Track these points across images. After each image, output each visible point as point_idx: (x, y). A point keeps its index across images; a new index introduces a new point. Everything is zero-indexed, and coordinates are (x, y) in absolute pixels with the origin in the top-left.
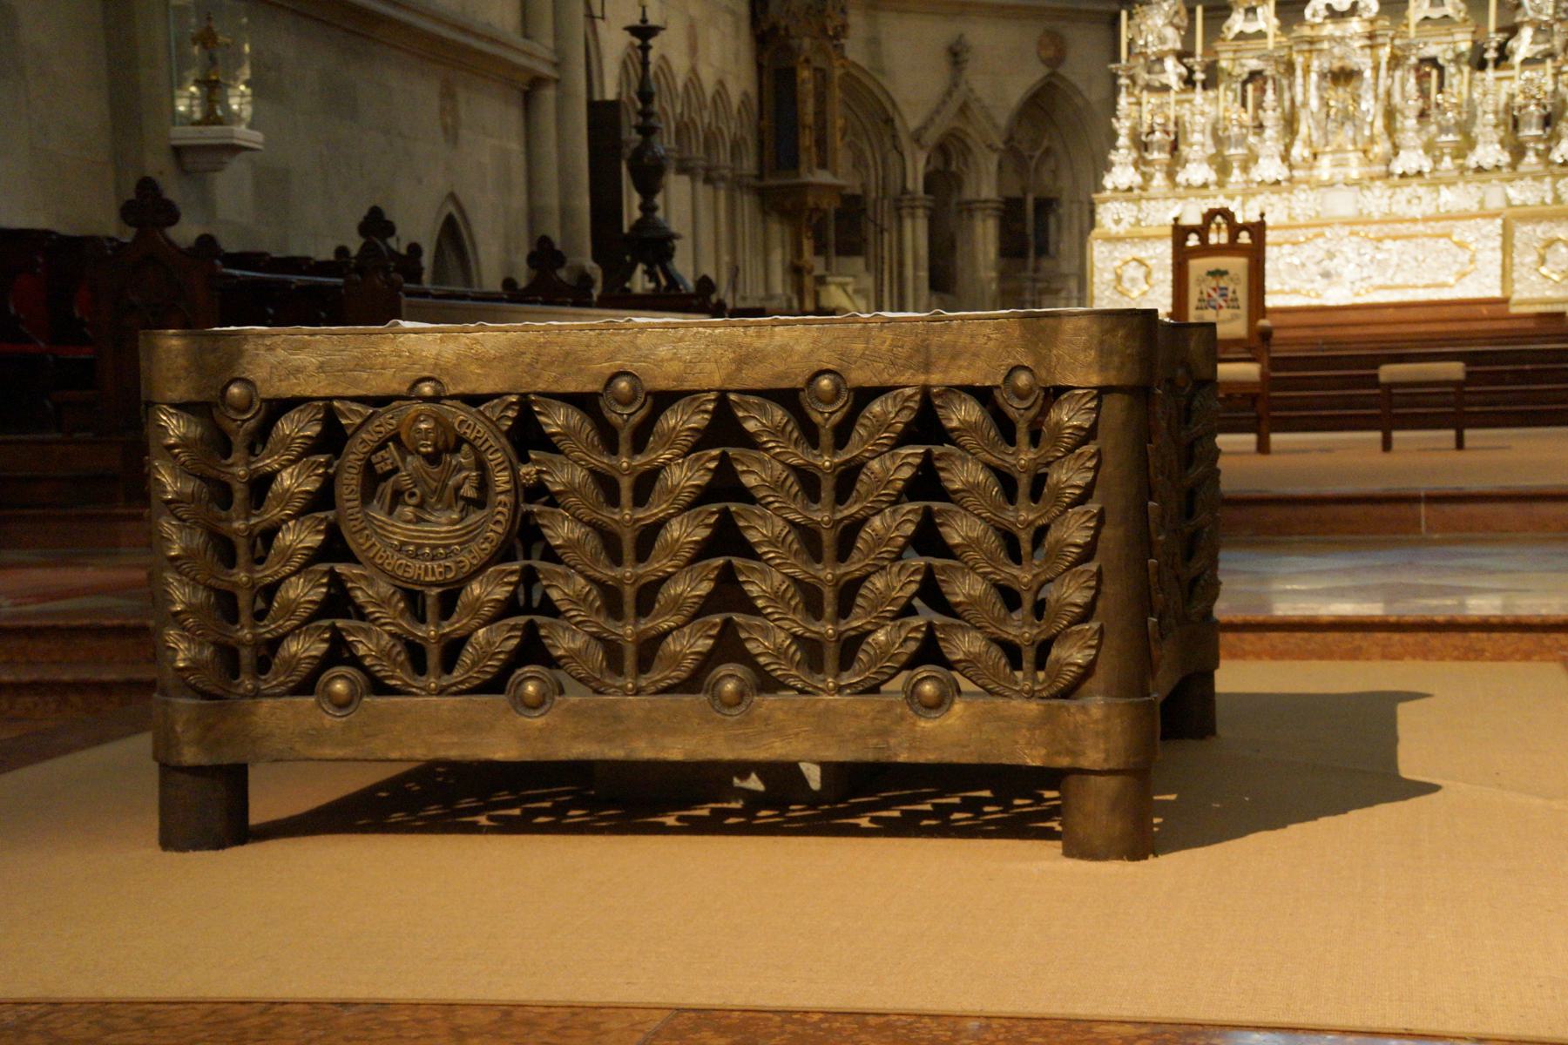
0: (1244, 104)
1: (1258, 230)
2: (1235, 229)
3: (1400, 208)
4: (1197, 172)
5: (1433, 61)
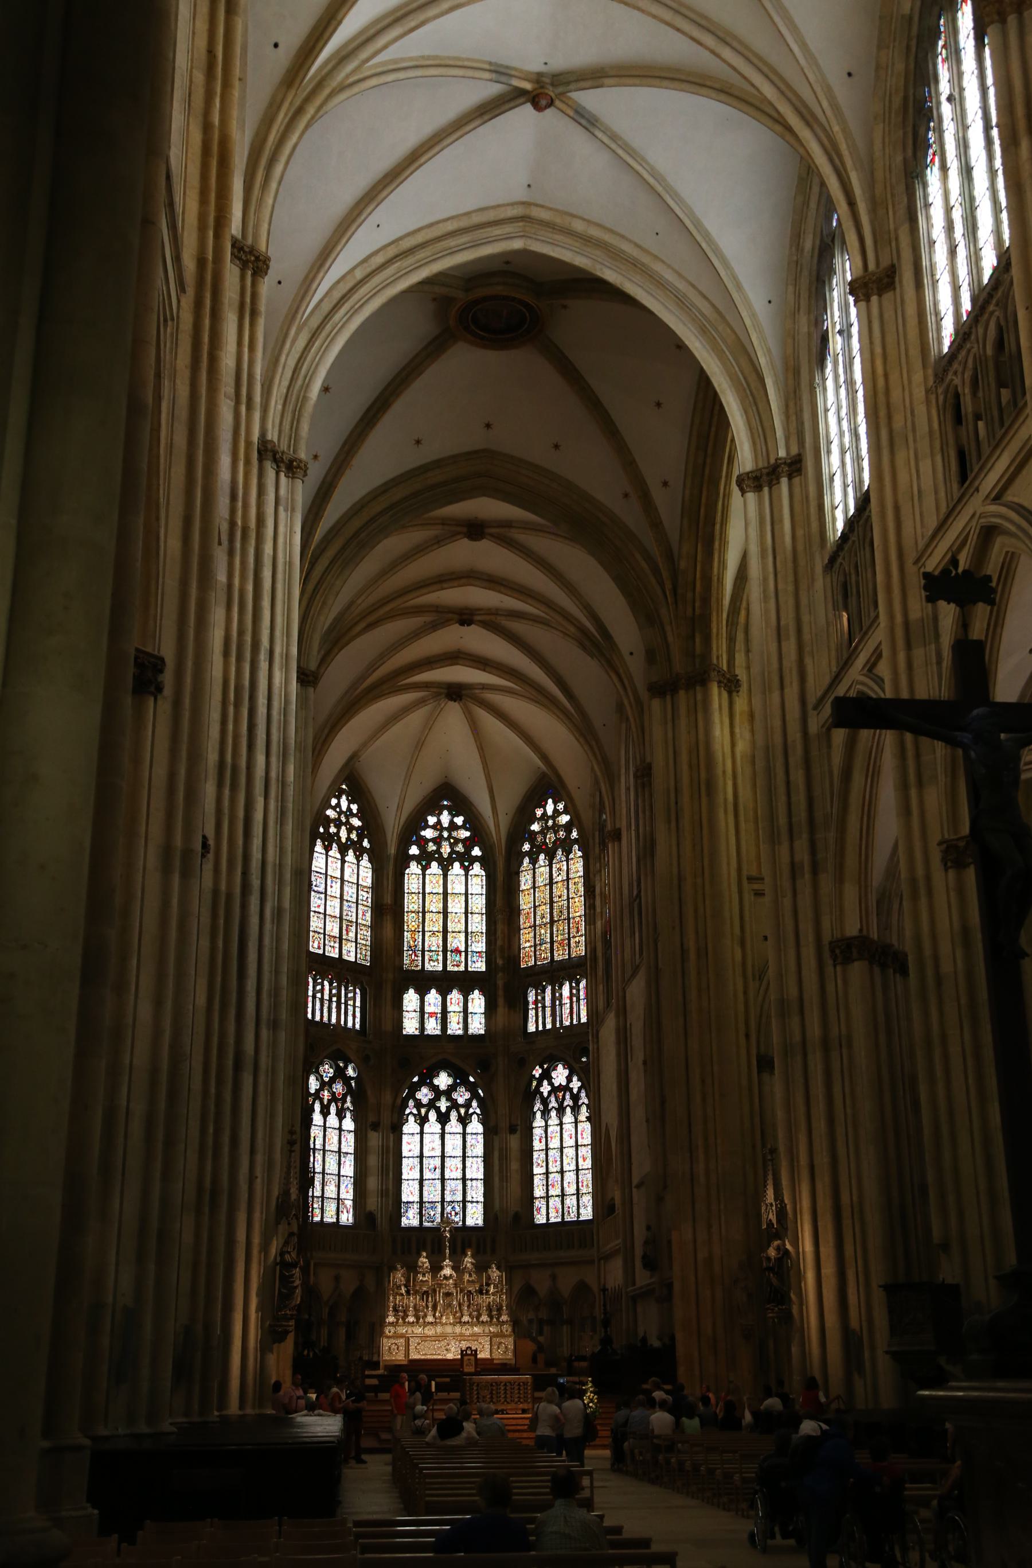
0: (423, 1300)
1: (476, 1351)
2: (472, 1351)
3: (464, 1331)
4: (411, 1319)
5: (470, 1291)
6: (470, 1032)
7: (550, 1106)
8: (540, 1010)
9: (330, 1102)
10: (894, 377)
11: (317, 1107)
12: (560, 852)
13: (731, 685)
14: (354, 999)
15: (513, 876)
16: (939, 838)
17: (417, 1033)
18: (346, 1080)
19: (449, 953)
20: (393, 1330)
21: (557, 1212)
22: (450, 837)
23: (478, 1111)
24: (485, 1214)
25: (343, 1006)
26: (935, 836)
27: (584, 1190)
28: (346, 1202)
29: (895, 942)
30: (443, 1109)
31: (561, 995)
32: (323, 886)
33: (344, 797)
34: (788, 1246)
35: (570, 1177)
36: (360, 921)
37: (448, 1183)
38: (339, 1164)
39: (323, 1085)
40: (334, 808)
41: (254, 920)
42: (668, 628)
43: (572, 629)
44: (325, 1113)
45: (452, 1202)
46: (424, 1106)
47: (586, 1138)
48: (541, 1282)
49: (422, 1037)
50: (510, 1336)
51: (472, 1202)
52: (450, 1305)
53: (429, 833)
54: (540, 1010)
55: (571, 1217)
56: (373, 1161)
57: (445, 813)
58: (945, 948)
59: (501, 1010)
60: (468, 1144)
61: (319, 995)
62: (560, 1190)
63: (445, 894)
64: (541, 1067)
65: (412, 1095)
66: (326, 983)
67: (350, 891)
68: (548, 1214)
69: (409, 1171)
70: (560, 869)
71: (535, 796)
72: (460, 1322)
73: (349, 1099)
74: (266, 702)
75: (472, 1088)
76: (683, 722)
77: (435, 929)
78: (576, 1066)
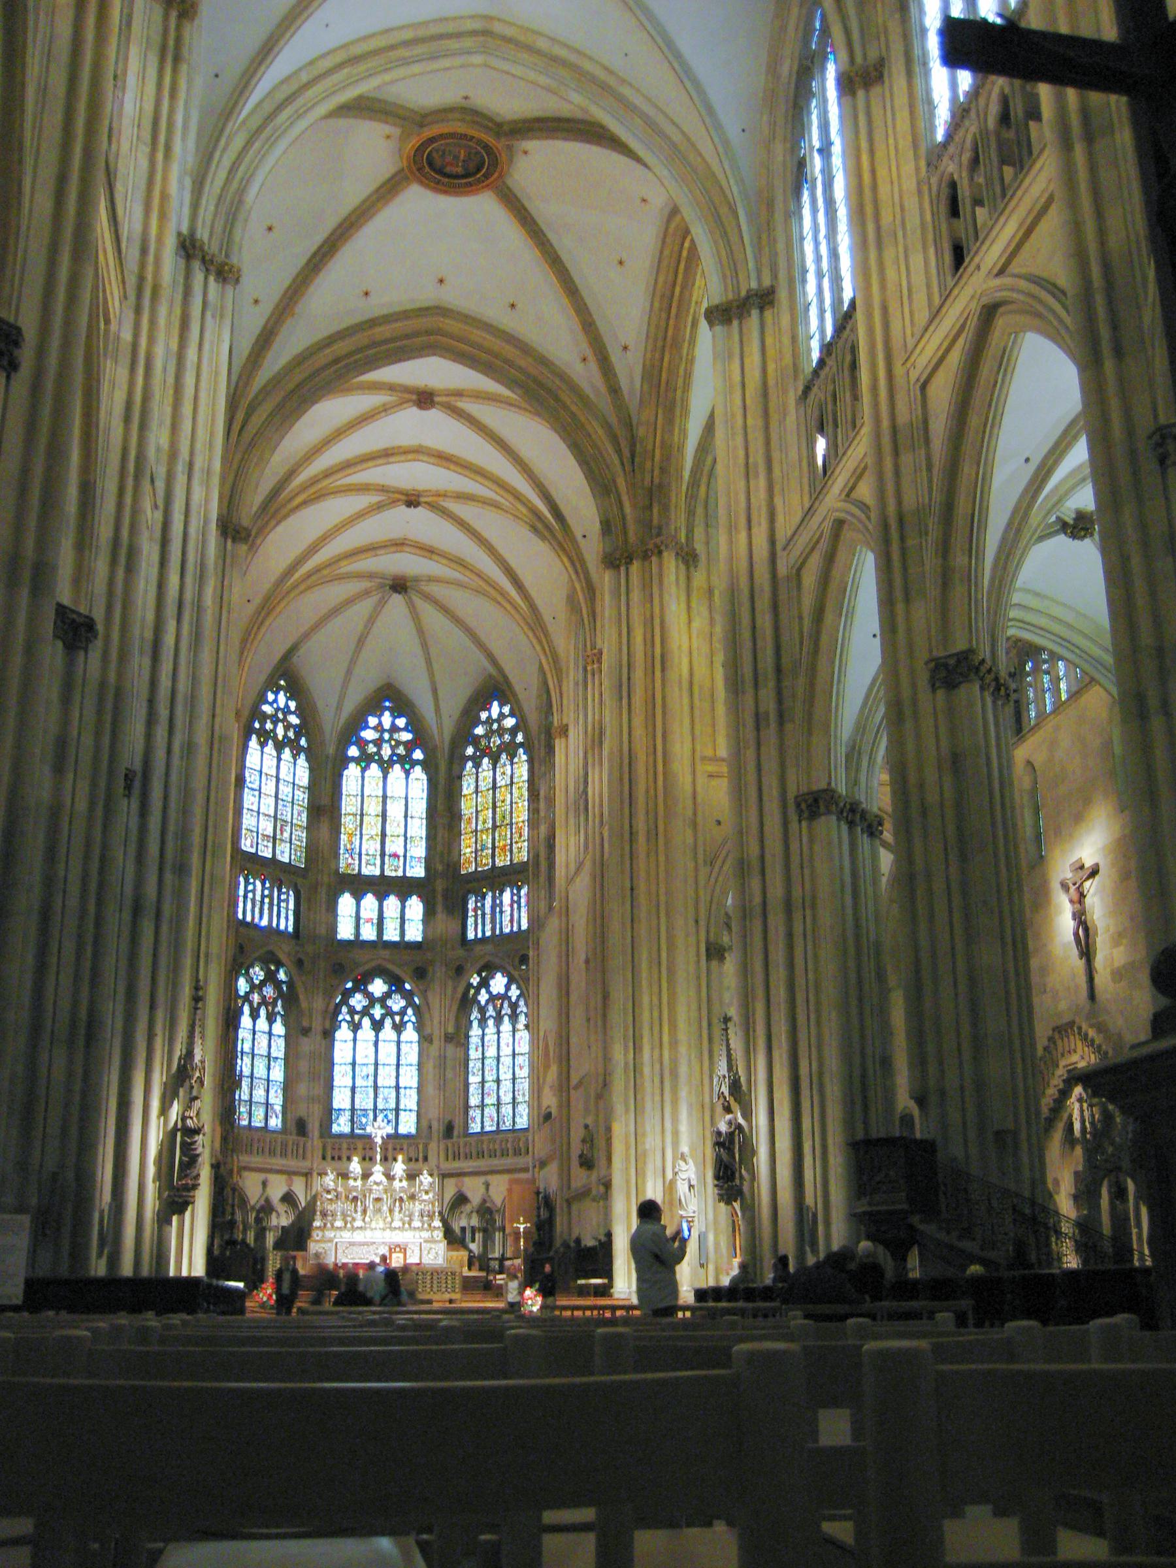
4: (339, 1223)
6: (407, 938)
7: (488, 1015)
8: (479, 918)
9: (259, 1005)
10: (882, 172)
11: (246, 1009)
12: (504, 756)
13: (689, 558)
14: (287, 901)
15: (455, 780)
16: (926, 656)
17: (352, 938)
18: (277, 984)
19: (387, 858)
20: (320, 1234)
22: (391, 738)
23: (413, 1019)
24: (418, 1122)
25: (275, 908)
26: (922, 655)
27: (520, 1099)
28: (276, 1107)
29: (863, 799)
30: (378, 1017)
31: (501, 902)
32: (258, 783)
33: (282, 693)
34: (741, 1120)
35: (506, 1086)
36: (295, 821)
37: (380, 1091)
38: (269, 1069)
39: (253, 987)
40: (271, 704)
41: (160, 755)
42: (625, 498)
43: (524, 511)
44: (255, 1016)
46: (357, 1013)
47: (524, 1046)
48: (474, 1189)
49: (357, 943)
50: (440, 1242)
52: (379, 1210)
53: (369, 735)
54: (479, 918)
55: (508, 1125)
56: (303, 1066)
57: (387, 713)
58: (931, 775)
59: (441, 916)
60: (402, 1053)
61: (250, 895)
63: (385, 797)
64: (479, 975)
65: (345, 1001)
66: (258, 884)
67: (285, 790)
68: (482, 1122)
69: (342, 1078)
70: (504, 773)
71: (481, 699)
72: (390, 1228)
73: (279, 1003)
74: (182, 517)
75: (408, 996)
76: (636, 595)
77: (373, 833)
78: (516, 974)
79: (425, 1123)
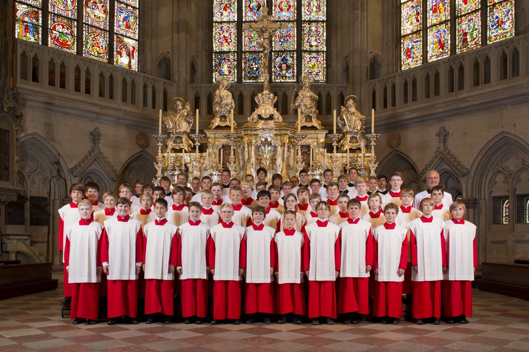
21: (442, 46)
28: (126, 40)
45: (283, 52)
51: (310, 52)
62: (448, 13)
79: (338, 67)
